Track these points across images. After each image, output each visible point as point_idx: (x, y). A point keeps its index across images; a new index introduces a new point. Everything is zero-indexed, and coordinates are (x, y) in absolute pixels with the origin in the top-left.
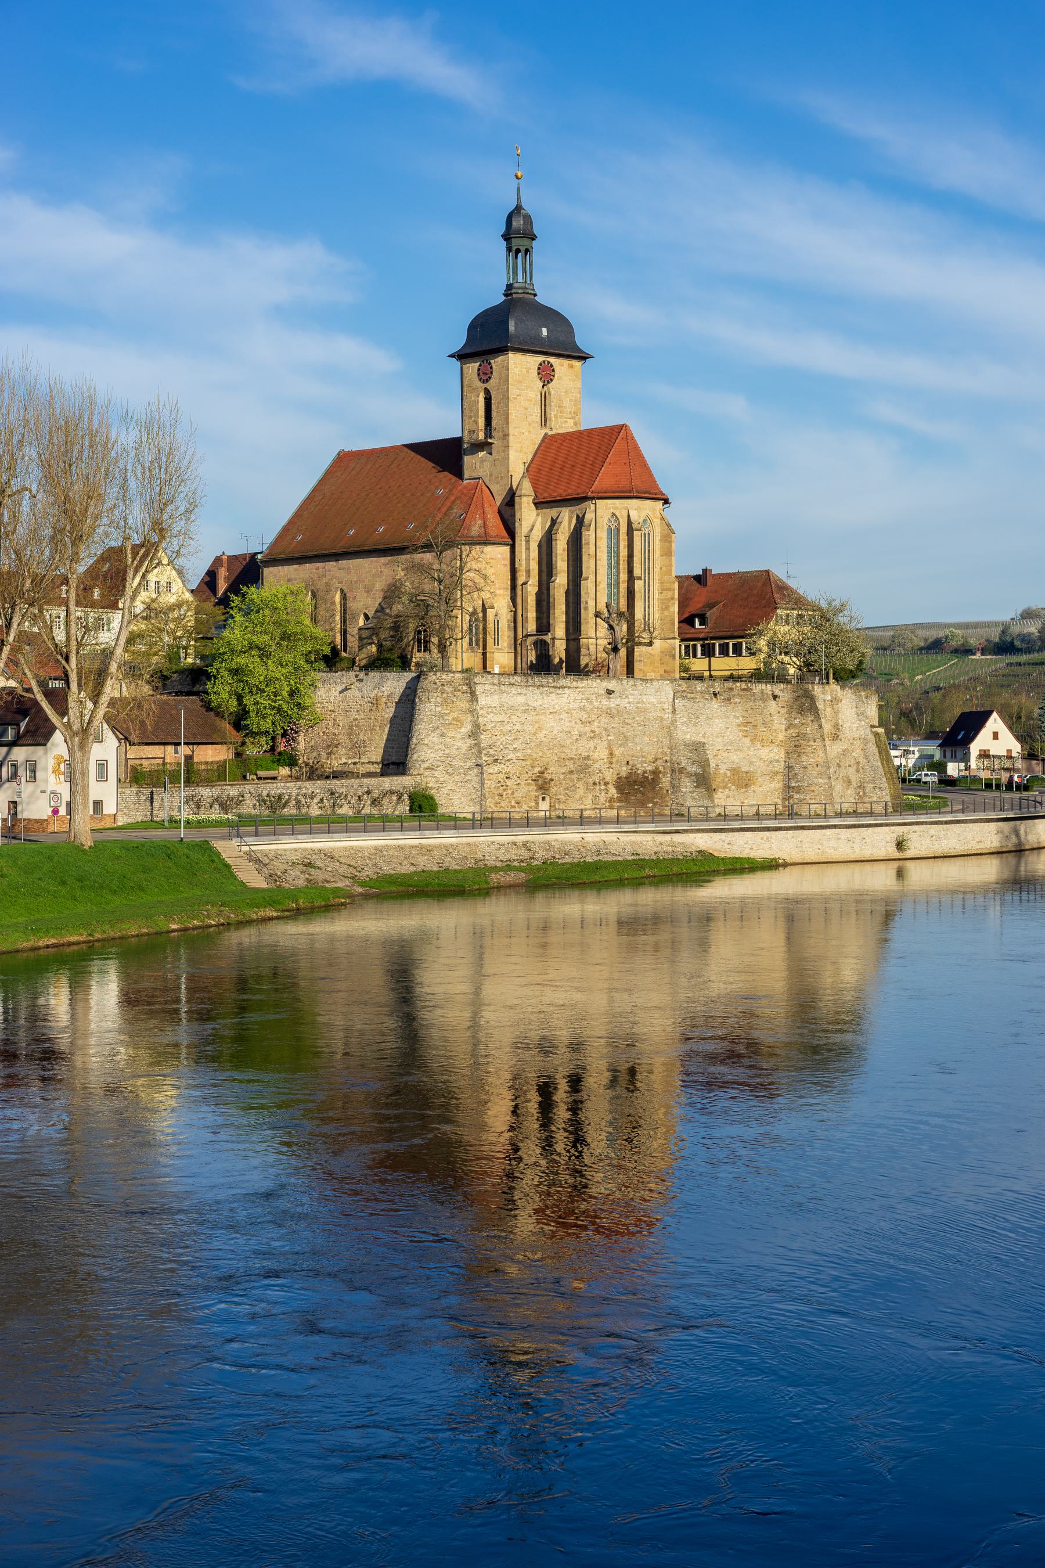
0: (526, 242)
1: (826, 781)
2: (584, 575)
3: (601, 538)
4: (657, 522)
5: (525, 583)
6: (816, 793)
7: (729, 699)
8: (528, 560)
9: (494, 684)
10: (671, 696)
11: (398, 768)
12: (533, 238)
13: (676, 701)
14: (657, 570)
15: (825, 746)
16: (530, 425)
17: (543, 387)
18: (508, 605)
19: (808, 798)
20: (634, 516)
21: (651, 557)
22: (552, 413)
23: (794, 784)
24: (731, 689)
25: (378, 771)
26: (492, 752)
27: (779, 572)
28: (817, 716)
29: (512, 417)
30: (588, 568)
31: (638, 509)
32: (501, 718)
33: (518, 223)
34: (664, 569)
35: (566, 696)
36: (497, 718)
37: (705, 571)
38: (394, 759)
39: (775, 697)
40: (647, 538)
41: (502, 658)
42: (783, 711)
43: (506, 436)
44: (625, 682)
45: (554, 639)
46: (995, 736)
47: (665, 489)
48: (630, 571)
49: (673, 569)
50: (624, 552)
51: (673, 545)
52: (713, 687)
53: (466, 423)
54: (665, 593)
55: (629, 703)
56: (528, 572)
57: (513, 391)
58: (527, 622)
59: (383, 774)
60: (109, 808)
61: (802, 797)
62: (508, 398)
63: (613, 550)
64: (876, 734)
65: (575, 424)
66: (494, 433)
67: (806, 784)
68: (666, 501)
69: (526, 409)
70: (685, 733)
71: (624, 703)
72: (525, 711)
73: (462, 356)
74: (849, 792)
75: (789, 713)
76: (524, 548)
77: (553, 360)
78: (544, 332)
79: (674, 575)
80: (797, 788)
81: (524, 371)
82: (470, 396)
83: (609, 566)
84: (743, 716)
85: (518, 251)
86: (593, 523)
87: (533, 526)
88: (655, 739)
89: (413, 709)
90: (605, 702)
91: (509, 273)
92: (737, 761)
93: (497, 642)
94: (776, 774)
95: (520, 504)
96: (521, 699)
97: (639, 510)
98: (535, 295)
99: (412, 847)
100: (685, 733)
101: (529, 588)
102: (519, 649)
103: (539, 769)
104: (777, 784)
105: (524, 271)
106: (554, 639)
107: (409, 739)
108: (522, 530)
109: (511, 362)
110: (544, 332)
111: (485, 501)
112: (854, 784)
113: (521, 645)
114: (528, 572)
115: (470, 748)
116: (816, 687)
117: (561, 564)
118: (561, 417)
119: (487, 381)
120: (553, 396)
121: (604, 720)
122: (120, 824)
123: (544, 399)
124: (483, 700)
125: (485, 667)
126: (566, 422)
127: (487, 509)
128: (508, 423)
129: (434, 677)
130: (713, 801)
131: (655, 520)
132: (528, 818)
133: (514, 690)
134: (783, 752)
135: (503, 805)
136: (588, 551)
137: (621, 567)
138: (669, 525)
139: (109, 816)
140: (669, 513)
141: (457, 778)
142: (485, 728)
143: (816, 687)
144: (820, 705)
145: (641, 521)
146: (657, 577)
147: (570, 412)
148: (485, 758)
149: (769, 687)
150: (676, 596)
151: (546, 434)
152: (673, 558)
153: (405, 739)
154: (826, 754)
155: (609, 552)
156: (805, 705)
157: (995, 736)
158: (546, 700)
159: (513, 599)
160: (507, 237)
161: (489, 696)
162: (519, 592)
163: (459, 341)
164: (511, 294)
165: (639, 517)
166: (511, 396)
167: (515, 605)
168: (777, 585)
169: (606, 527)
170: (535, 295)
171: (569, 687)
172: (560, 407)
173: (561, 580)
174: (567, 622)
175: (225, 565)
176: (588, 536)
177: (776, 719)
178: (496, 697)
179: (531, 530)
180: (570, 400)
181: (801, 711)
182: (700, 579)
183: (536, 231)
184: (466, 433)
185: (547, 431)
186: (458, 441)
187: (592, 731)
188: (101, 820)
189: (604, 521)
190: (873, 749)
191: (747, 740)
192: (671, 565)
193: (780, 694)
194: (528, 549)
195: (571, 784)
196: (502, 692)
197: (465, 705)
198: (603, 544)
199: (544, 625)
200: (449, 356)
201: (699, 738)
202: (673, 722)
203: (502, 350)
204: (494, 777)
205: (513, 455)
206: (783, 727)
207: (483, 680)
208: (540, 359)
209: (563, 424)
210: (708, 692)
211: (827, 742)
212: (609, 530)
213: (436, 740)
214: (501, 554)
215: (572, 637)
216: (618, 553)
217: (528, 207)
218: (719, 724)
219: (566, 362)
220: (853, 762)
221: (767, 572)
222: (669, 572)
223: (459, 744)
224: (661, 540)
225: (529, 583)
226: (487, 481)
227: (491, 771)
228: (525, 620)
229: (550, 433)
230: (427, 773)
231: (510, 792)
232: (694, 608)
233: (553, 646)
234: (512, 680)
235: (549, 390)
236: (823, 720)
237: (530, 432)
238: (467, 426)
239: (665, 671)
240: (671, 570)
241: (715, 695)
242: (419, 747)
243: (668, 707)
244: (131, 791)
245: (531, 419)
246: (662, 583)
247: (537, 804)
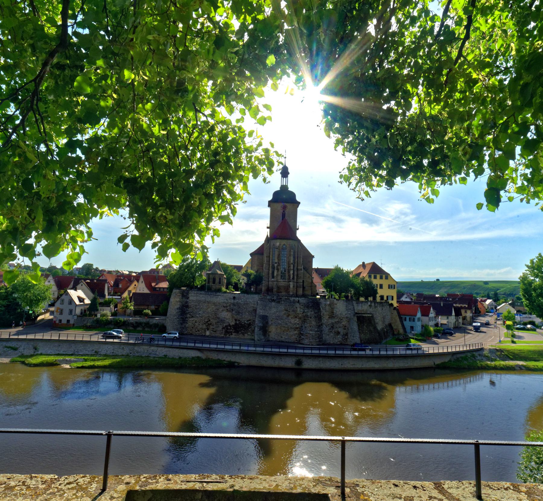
71: (240, 301)
72: (205, 302)
90: (232, 301)
94: (297, 328)
124: (191, 298)
133: (201, 296)
177: (299, 309)
178: (195, 298)
191: (285, 316)
201: (266, 314)
206: (302, 312)
218: (274, 310)
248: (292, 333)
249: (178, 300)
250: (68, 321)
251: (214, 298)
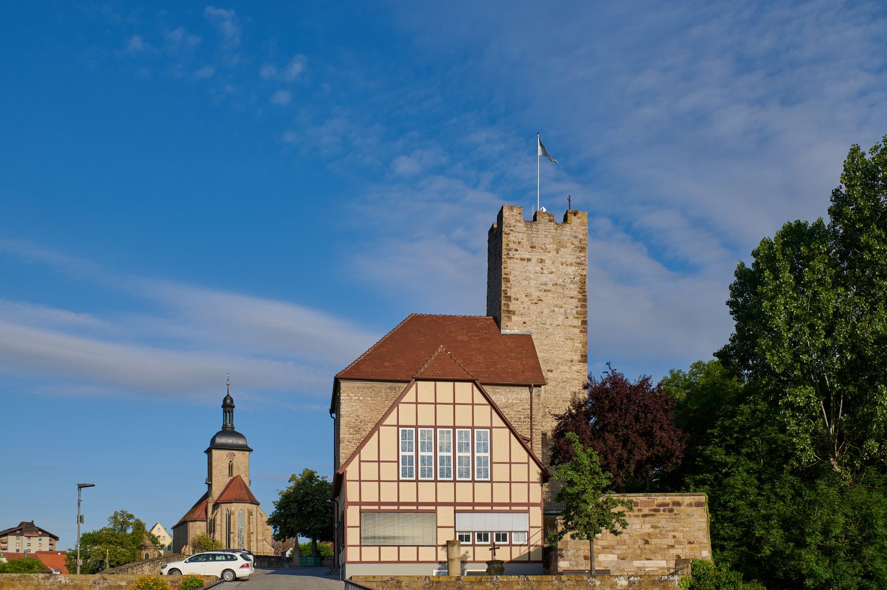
0: (231, 409)
16: (223, 476)
33: (228, 401)
68: (257, 504)
69: (221, 470)
77: (234, 452)
172: (238, 469)
208: (228, 452)
212: (226, 515)
219: (241, 452)
237: (223, 479)
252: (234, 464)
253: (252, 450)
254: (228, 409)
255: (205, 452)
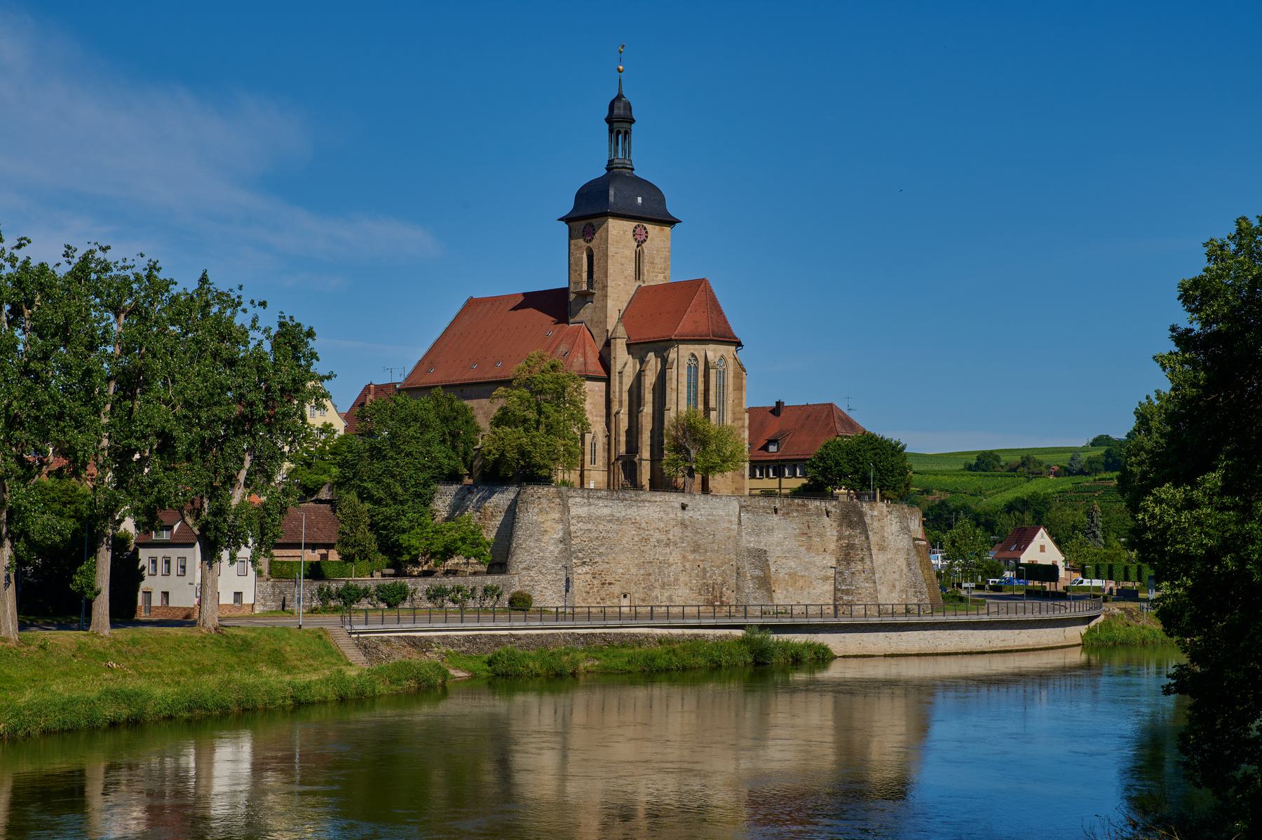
0: (626, 125)
1: (872, 585)
2: (667, 407)
3: (682, 374)
4: (731, 361)
5: (618, 413)
6: (863, 595)
7: (788, 514)
8: (621, 392)
9: (583, 497)
10: (738, 510)
11: (501, 568)
12: (632, 121)
13: (742, 514)
14: (730, 402)
15: (871, 555)
17: (638, 246)
18: (604, 430)
19: (855, 599)
20: (710, 355)
21: (725, 391)
22: (646, 268)
23: (843, 588)
24: (791, 505)
25: (485, 570)
26: (580, 555)
27: (842, 406)
28: (865, 532)
29: (610, 271)
30: (671, 400)
31: (714, 350)
32: (589, 526)
33: (619, 111)
34: (736, 401)
35: (646, 508)
36: (585, 527)
37: (778, 403)
38: (498, 560)
39: (828, 513)
40: (722, 375)
41: (596, 477)
42: (835, 524)
43: (605, 287)
44: (697, 497)
45: (641, 460)
46: (1042, 549)
47: (738, 333)
48: (706, 403)
49: (744, 401)
50: (701, 387)
51: (744, 381)
52: (774, 503)
53: (572, 276)
54: (736, 422)
55: (701, 515)
56: (621, 402)
57: (612, 250)
58: (619, 445)
59: (489, 573)
60: (248, 599)
61: (850, 598)
62: (607, 256)
63: (692, 385)
64: (916, 546)
65: (665, 278)
66: (595, 285)
67: (854, 588)
68: (738, 344)
69: (622, 264)
70: (750, 542)
71: (697, 515)
72: (610, 521)
73: (567, 219)
74: (893, 595)
75: (840, 525)
76: (617, 382)
78: (640, 200)
79: (746, 406)
80: (847, 592)
81: (622, 233)
82: (576, 253)
83: (689, 399)
84: (799, 528)
85: (618, 133)
86: (676, 361)
87: (626, 364)
88: (723, 547)
89: (514, 518)
90: (680, 513)
91: (610, 150)
92: (794, 566)
93: (593, 461)
94: (826, 579)
95: (615, 345)
96: (606, 511)
97: (713, 352)
98: (633, 169)
99: (503, 635)
100: (750, 542)
101: (621, 416)
102: (612, 467)
103: (622, 571)
104: (829, 587)
105: (624, 149)
106: (641, 460)
107: (510, 544)
108: (617, 366)
109: (610, 225)
110: (640, 200)
111: (587, 342)
112: (897, 588)
113: (613, 464)
114: (621, 402)
115: (561, 552)
116: (864, 505)
117: (648, 396)
118: (653, 272)
119: (590, 241)
120: (646, 254)
121: (677, 530)
122: (256, 612)
123: (639, 257)
124: (574, 511)
125: (582, 483)
126: (657, 276)
127: (588, 348)
128: (607, 276)
129: (532, 491)
130: (771, 599)
131: (729, 360)
132: (589, 612)
133: (601, 503)
134: (835, 560)
135: (589, 600)
136: (671, 385)
137: (699, 399)
138: (740, 365)
139: (248, 605)
140: (741, 355)
141: (549, 577)
142: (575, 535)
143: (864, 505)
144: (868, 520)
145: (717, 360)
146: (730, 408)
147: (661, 268)
148: (574, 561)
149: (823, 504)
150: (747, 422)
151: (640, 286)
152: (744, 393)
153: (507, 543)
154: (872, 562)
155: (689, 387)
156: (853, 520)
157: (1042, 549)
158: (629, 512)
159: (608, 424)
160: (609, 120)
161: (578, 507)
162: (613, 419)
163: (568, 207)
164: (612, 169)
165: (715, 357)
166: (610, 254)
167: (609, 430)
168: (839, 418)
169: (686, 365)
170: (633, 169)
171: (649, 501)
173: (648, 409)
174: (652, 445)
175: (372, 392)
176: (672, 374)
178: (586, 509)
179: (624, 367)
180: (661, 258)
181: (851, 525)
182: (777, 409)
183: (635, 116)
184: (572, 285)
185: (640, 283)
186: (565, 291)
187: (668, 539)
188: (240, 608)
189: (685, 361)
190: (914, 558)
191: (803, 549)
192: (742, 398)
193: (833, 510)
194: (621, 383)
195: (649, 584)
196: (590, 505)
197: (557, 516)
198: (684, 380)
199: (633, 447)
200: (560, 220)
201: (762, 546)
202: (739, 534)
203: (606, 215)
204: (582, 577)
205: (610, 303)
207: (574, 494)
208: (635, 224)
209: (655, 277)
210: (769, 508)
211: (874, 551)
212: (689, 367)
213: (532, 544)
214: (598, 387)
215: (656, 458)
216: (696, 387)
217: (628, 96)
218: (778, 536)
220: (897, 569)
221: (831, 405)
222: (740, 404)
223: (552, 548)
224: (734, 377)
225: (622, 411)
226: (589, 325)
227: (579, 571)
228: (617, 442)
229: (643, 285)
230: (524, 573)
231: (595, 590)
232: (770, 434)
233: (640, 466)
234: (599, 495)
235: (642, 249)
236: (869, 533)
237: (625, 284)
238: (573, 279)
239: (736, 489)
240: (741, 403)
241: (776, 511)
242: (518, 551)
243: (735, 520)
244: (267, 586)
245: (626, 273)
246: (734, 413)
247: (619, 600)
248: (818, 591)
249: (557, 516)
250: (238, 595)
251: (635, 509)
252: (646, 251)
253: (680, 222)
254: (623, 126)
255: (560, 220)
